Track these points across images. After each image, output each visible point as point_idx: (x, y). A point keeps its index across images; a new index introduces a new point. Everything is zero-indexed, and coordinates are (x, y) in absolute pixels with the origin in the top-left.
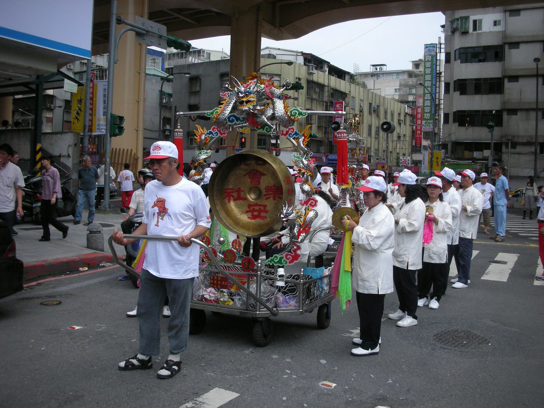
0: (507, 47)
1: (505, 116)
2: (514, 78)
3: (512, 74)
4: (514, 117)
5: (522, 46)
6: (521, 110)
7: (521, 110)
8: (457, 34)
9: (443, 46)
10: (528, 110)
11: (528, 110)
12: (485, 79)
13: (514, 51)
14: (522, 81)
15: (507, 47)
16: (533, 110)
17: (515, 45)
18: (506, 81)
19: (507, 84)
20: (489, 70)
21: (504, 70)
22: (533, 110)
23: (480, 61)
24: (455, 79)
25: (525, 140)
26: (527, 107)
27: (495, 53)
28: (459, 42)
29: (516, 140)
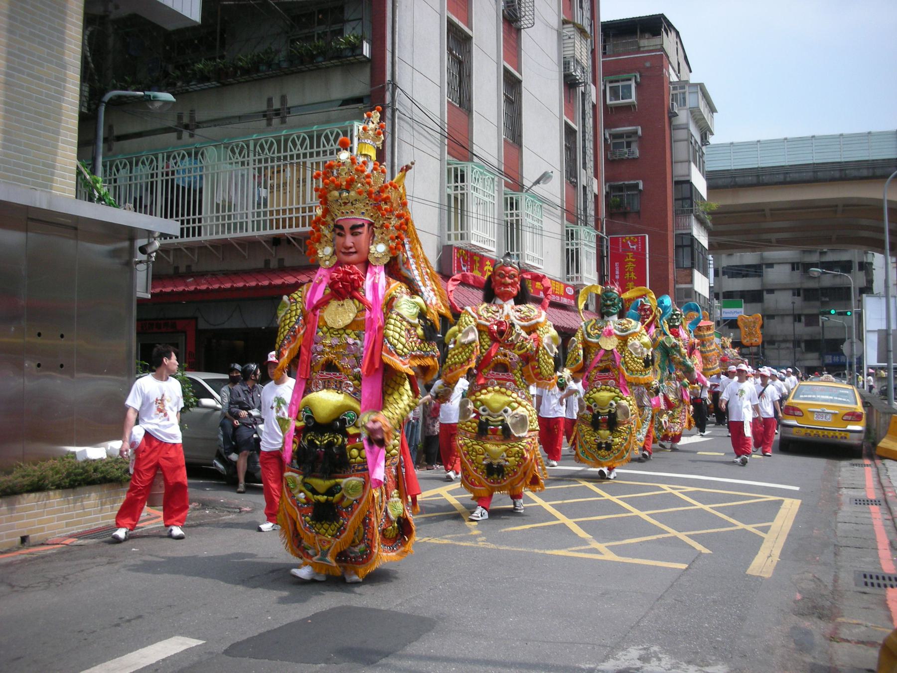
2: (771, 291)
3: (769, 287)
4: (772, 321)
5: (775, 266)
6: (778, 315)
7: (778, 315)
8: (724, 256)
9: (711, 262)
11: (783, 315)
12: (748, 291)
13: (769, 270)
16: (787, 315)
17: (770, 265)
18: (765, 293)
19: (766, 296)
20: (749, 284)
21: (763, 284)
22: (787, 315)
23: (743, 276)
24: (725, 290)
25: (781, 339)
27: (755, 270)
28: (726, 261)
29: (775, 338)
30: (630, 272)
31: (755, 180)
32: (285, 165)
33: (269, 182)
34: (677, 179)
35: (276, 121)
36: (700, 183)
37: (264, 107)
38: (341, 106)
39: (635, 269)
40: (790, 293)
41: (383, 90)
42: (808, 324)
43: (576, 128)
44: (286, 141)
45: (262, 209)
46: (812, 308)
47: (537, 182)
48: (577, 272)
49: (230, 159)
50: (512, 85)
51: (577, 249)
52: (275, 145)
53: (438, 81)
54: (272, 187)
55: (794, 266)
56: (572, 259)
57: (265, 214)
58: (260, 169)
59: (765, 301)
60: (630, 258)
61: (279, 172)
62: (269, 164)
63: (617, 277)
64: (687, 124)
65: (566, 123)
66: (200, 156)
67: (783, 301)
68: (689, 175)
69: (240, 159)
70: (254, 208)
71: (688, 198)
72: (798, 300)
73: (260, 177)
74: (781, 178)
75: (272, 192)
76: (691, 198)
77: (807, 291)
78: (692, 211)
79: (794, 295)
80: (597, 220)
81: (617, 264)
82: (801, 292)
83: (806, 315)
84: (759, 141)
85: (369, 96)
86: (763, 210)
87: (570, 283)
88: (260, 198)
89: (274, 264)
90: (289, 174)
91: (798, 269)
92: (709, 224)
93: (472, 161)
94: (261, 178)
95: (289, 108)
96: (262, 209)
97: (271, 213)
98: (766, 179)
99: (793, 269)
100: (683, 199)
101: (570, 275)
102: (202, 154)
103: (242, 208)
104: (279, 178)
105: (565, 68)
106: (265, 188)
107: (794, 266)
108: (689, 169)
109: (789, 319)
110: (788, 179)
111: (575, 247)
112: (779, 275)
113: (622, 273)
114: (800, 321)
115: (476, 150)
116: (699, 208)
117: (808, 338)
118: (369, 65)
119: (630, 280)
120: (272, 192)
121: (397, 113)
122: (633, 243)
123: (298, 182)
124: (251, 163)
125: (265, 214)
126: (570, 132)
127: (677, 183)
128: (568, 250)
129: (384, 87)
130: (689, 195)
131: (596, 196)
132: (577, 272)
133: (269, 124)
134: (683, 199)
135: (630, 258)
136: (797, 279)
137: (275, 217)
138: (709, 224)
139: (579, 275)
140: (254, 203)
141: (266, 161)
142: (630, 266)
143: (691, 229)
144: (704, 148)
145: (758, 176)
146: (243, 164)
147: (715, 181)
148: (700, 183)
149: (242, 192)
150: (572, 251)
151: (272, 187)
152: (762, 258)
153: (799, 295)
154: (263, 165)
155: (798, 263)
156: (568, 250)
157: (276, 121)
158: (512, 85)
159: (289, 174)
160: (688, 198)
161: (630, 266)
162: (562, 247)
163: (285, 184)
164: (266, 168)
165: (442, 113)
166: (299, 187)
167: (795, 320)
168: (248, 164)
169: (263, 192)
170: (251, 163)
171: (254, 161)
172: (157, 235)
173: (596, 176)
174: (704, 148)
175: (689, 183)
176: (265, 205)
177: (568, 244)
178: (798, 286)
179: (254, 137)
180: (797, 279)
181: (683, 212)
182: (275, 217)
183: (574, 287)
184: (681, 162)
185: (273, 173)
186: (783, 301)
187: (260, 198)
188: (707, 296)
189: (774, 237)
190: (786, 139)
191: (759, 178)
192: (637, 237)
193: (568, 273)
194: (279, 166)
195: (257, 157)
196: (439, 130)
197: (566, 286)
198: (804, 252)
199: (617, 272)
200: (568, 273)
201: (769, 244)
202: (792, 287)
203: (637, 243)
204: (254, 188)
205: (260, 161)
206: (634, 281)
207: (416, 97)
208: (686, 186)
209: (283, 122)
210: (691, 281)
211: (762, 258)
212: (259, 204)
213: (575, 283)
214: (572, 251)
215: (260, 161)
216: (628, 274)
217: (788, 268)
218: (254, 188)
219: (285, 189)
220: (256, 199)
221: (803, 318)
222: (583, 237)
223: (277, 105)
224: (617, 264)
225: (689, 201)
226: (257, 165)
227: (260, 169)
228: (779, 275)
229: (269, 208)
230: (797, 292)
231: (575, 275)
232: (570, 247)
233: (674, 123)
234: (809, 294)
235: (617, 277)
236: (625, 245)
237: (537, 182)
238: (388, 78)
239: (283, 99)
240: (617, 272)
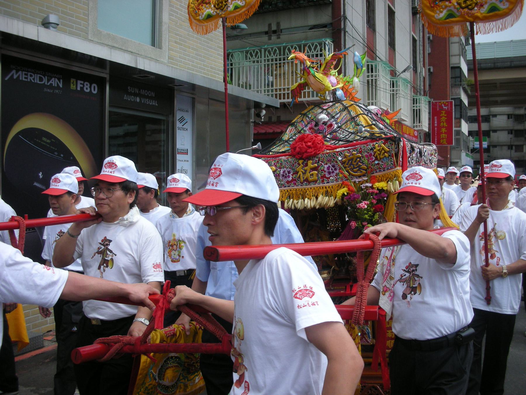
0: (491, 116)
1: (491, 149)
2: (495, 131)
3: (495, 129)
4: (495, 149)
5: (498, 116)
6: (499, 145)
7: (499, 145)
10: (502, 146)
11: (502, 146)
13: (494, 119)
14: (498, 133)
15: (491, 116)
17: (495, 116)
18: (491, 132)
19: (492, 134)
21: (490, 126)
26: (501, 144)
30: (443, 122)
31: (492, 65)
32: (284, 63)
33: (274, 72)
34: (452, 66)
35: (274, 37)
36: (464, 68)
37: (266, 29)
38: (309, 29)
39: (446, 120)
40: (506, 132)
41: (340, 20)
42: (516, 151)
43: (417, 38)
44: (284, 48)
45: (270, 88)
46: (518, 142)
47: (404, 71)
48: (419, 122)
49: (249, 59)
50: (391, 14)
51: (419, 109)
52: (278, 51)
53: (361, 14)
54: (276, 75)
55: (509, 116)
56: (416, 114)
57: (272, 91)
58: (268, 65)
59: (491, 137)
60: (443, 114)
61: (280, 67)
62: (274, 62)
63: (436, 125)
64: (458, 33)
65: (413, 36)
66: (230, 57)
67: (503, 137)
68: (459, 63)
69: (256, 59)
70: (265, 87)
71: (458, 77)
72: (511, 136)
73: (268, 69)
74: (508, 64)
75: (276, 78)
76: (460, 77)
77: (516, 131)
78: (461, 85)
79: (509, 133)
80: (424, 91)
81: (436, 118)
82: (513, 132)
83: (516, 146)
84: (495, 42)
85: (331, 24)
86: (496, 83)
87: (416, 129)
88: (269, 81)
89: (274, 119)
90: (286, 68)
91: (511, 118)
92: (469, 92)
93: (376, 60)
94: (268, 70)
95: (281, 30)
96: (270, 88)
97: (276, 90)
98: (499, 65)
99: (508, 118)
100: (455, 78)
101: (415, 124)
102: (232, 56)
103: (258, 88)
104: (280, 70)
105: (412, 4)
106: (272, 75)
107: (509, 116)
108: (460, 60)
109: (505, 148)
110: (513, 65)
111: (418, 108)
112: (500, 121)
113: (439, 122)
114: (512, 149)
115: (378, 53)
116: (465, 84)
117: (517, 159)
118: (331, 6)
119: (443, 127)
120: (276, 78)
121: (347, 34)
122: (445, 105)
123: (292, 72)
124: (263, 61)
125: (272, 91)
126: (414, 41)
127: (452, 68)
128: (414, 110)
129: (340, 19)
130: (459, 75)
131: (424, 78)
132: (419, 122)
133: (270, 39)
134: (455, 78)
135: (443, 114)
136: (510, 124)
137: (278, 92)
138: (469, 92)
139: (420, 124)
140: (265, 85)
141: (272, 60)
142: (443, 119)
143: (460, 95)
144: (466, 47)
145: (495, 63)
146: (258, 62)
147: (475, 66)
148: (464, 68)
149: (258, 77)
150: (417, 110)
151: (276, 75)
152: (490, 112)
153: (512, 133)
154: (270, 62)
155: (511, 115)
156: (414, 110)
157: (274, 37)
158: (391, 14)
159: (286, 68)
160: (458, 77)
161: (443, 119)
162: (411, 108)
163: (284, 74)
164: (272, 64)
165: (364, 32)
166: (293, 75)
167: (509, 149)
168: (261, 62)
169: (271, 79)
170: (263, 61)
171: (265, 60)
172: (264, 106)
173: (424, 66)
174: (466, 47)
175: (459, 68)
176: (272, 86)
177: (414, 107)
178: (511, 128)
179: (266, 47)
180: (510, 124)
181: (455, 85)
182: (278, 92)
183: (418, 131)
184: (455, 55)
185: (277, 67)
186: (503, 137)
187: (269, 81)
188: (467, 135)
189: (499, 99)
190: (512, 41)
191: (496, 65)
192: (448, 102)
193: (414, 123)
194: (280, 64)
195: (266, 58)
196: (361, 41)
197: (415, 130)
198: (515, 108)
199: (436, 122)
200: (414, 123)
201: (496, 104)
202: (507, 129)
203: (448, 105)
204: (265, 75)
205: (268, 60)
206: (446, 127)
207: (354, 24)
208: (457, 70)
209: (279, 38)
210: (460, 126)
211: (490, 112)
212: (268, 85)
213: (418, 129)
214: (417, 110)
215: (268, 60)
216: (442, 124)
217: (505, 117)
218: (265, 75)
219: (284, 77)
220: (267, 82)
221: (514, 147)
222: (423, 102)
223: (274, 28)
224: (436, 118)
225: (459, 79)
226: (267, 63)
227: (268, 65)
228: (500, 121)
229: (274, 87)
230: (510, 132)
231: (418, 124)
232: (415, 108)
233: (451, 33)
234: (518, 133)
235: (436, 125)
236: (441, 107)
237: (404, 71)
238: (342, 13)
239: (278, 24)
240: (436, 122)
